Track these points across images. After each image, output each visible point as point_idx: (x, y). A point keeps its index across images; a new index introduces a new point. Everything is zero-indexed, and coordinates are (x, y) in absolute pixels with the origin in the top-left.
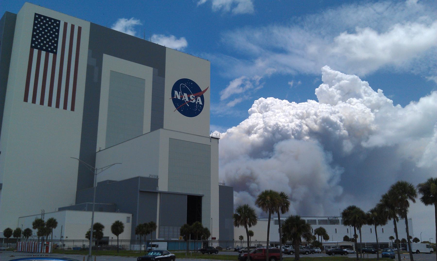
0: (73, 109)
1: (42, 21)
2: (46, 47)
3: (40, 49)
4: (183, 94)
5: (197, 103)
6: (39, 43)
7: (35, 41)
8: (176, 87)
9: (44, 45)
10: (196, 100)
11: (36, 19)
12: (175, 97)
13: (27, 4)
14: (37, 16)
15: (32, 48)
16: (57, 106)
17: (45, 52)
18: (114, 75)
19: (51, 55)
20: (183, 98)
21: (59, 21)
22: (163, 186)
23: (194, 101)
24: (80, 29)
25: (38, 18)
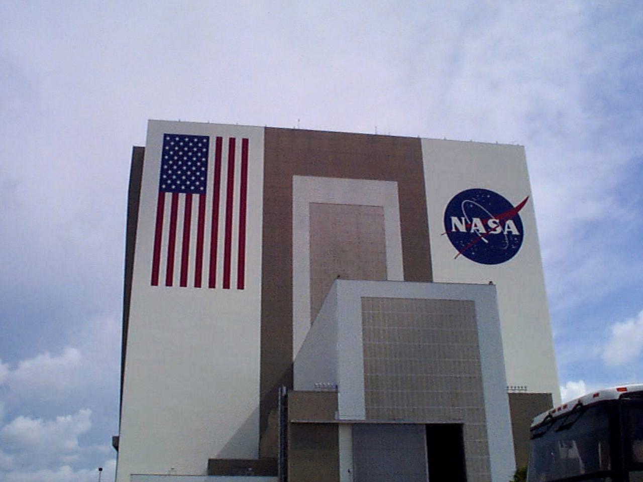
0: (241, 285)
1: (177, 144)
2: (185, 185)
4: (471, 221)
5: (505, 233)
7: (167, 180)
8: (454, 208)
9: (183, 182)
10: (504, 228)
11: (166, 143)
12: (454, 230)
14: (168, 138)
16: (212, 284)
17: (184, 195)
18: (316, 208)
19: (196, 197)
20: (473, 228)
21: (208, 138)
23: (499, 230)
24: (245, 142)
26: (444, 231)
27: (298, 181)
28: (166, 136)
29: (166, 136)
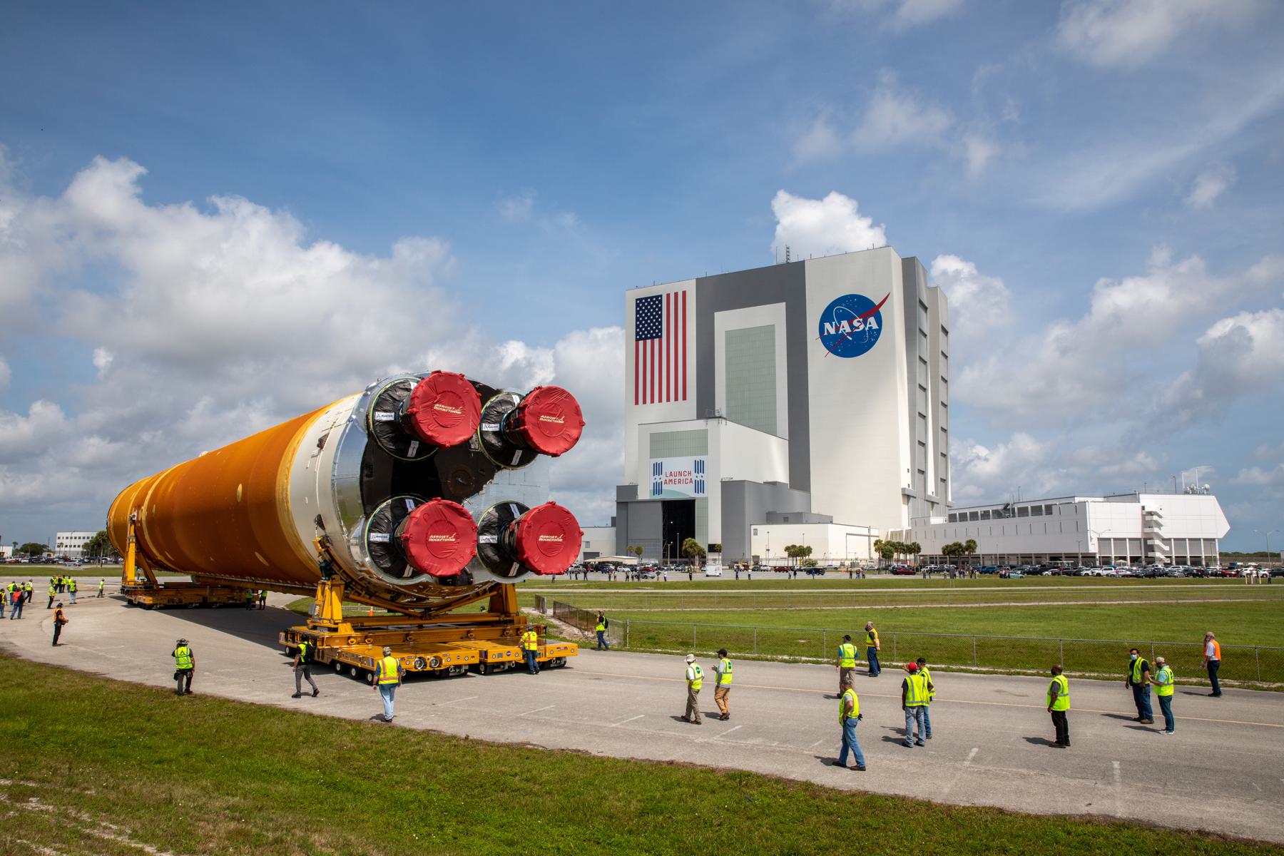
0: (684, 398)
8: (827, 317)
11: (637, 305)
15: (637, 340)
18: (730, 335)
19: (656, 341)
22: (644, 494)
23: (862, 327)
24: (684, 293)
27: (719, 316)
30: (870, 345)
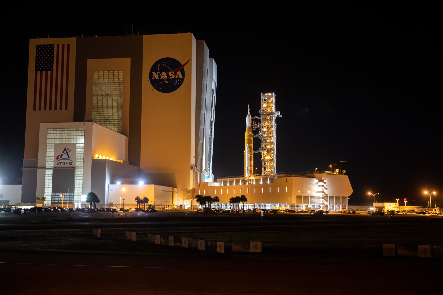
0: (66, 109)
3: (41, 71)
4: (161, 73)
6: (41, 66)
8: (154, 69)
9: (44, 66)
10: (176, 76)
11: (37, 49)
12: (153, 78)
13: (31, 40)
15: (36, 71)
19: (49, 73)
20: (162, 77)
21: (53, 45)
23: (173, 76)
24: (69, 45)
25: (39, 47)
26: (149, 79)
28: (37, 46)
29: (37, 46)
30: (178, 87)
